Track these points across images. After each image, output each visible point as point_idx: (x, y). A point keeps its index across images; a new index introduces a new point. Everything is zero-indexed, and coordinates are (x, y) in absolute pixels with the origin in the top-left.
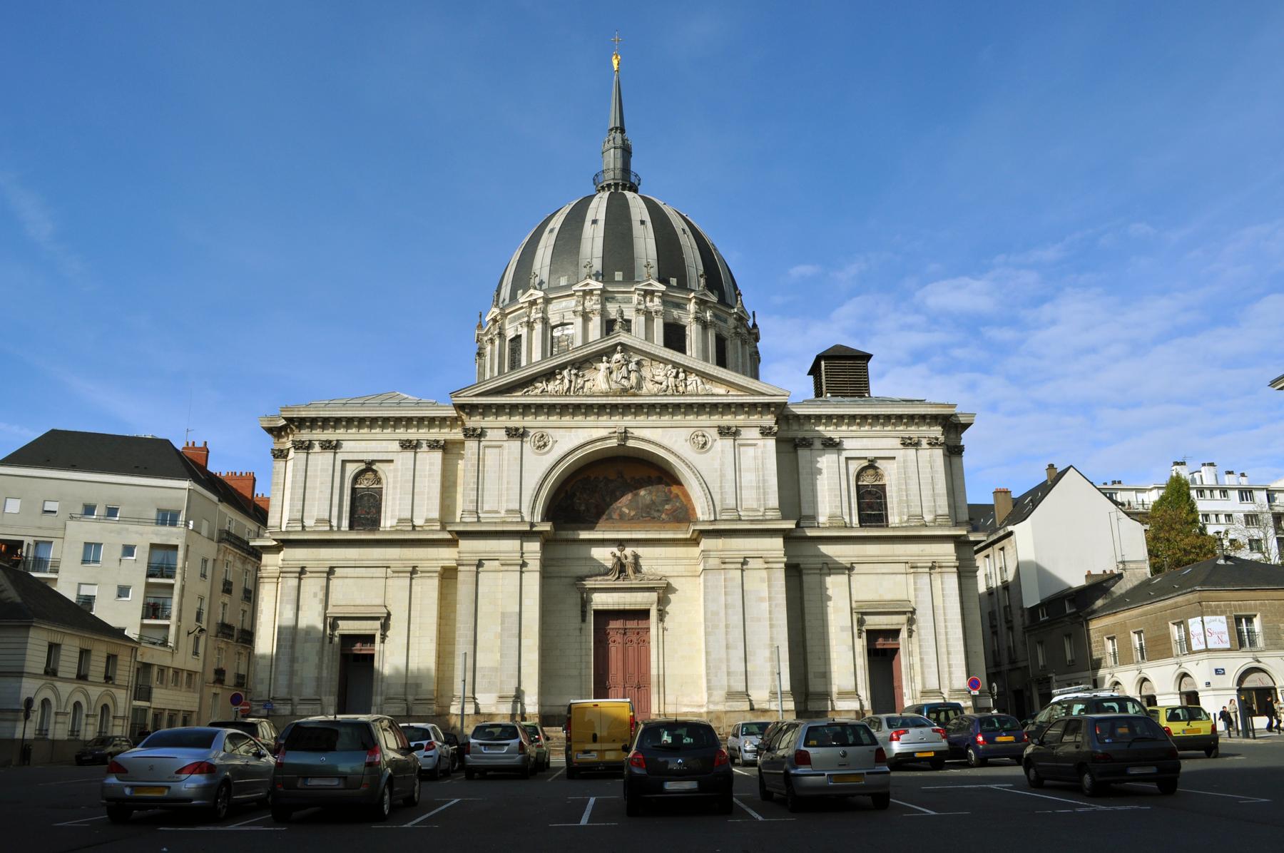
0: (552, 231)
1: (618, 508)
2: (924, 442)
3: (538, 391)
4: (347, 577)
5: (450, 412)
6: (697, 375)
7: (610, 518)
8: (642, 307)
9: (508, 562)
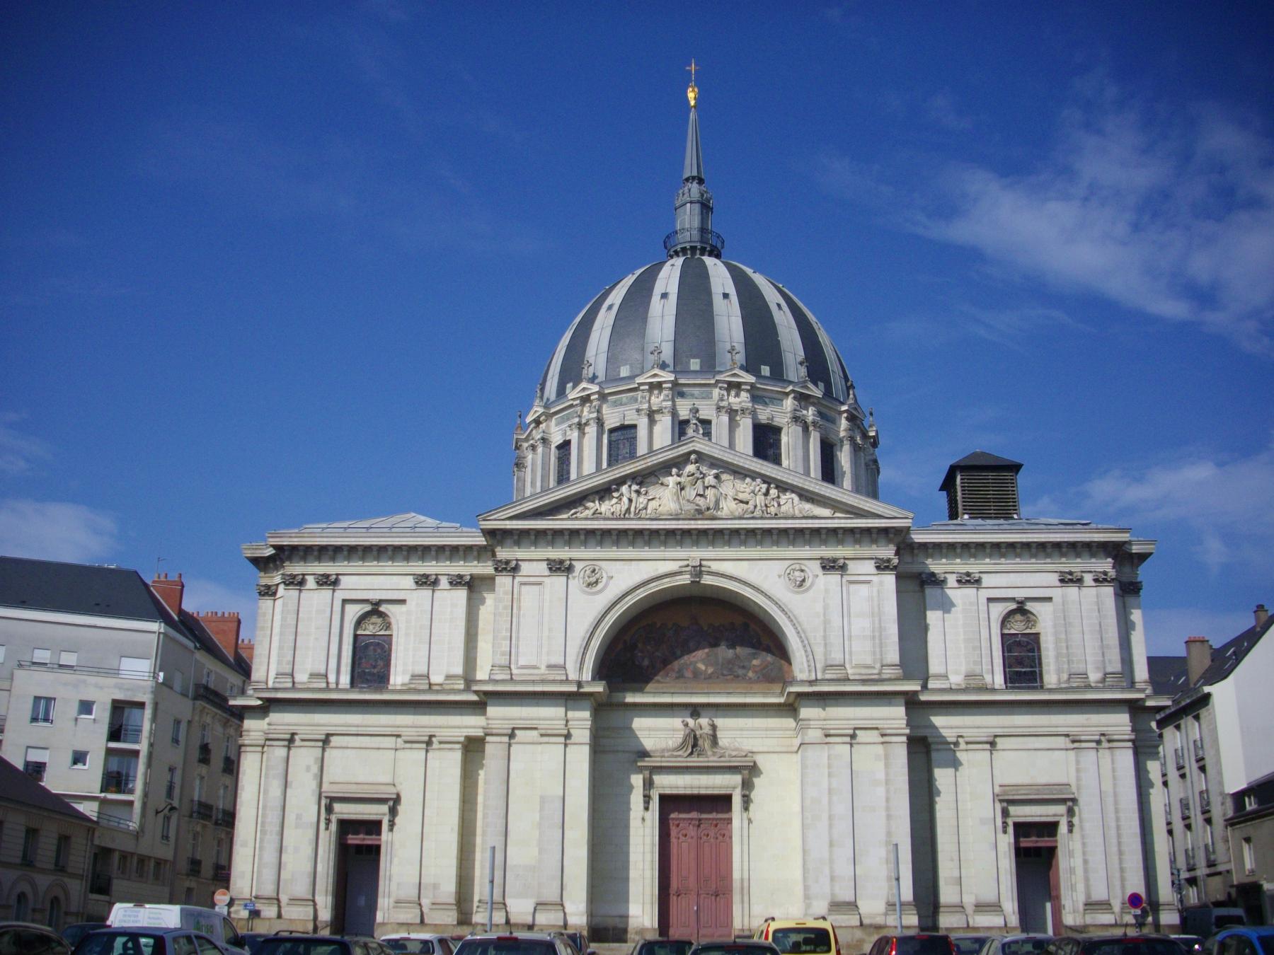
0: (610, 307)
1: (691, 663)
2: (1088, 579)
3: (588, 513)
4: (347, 748)
5: (478, 539)
6: (793, 492)
7: (680, 676)
8: (724, 404)
9: (549, 732)
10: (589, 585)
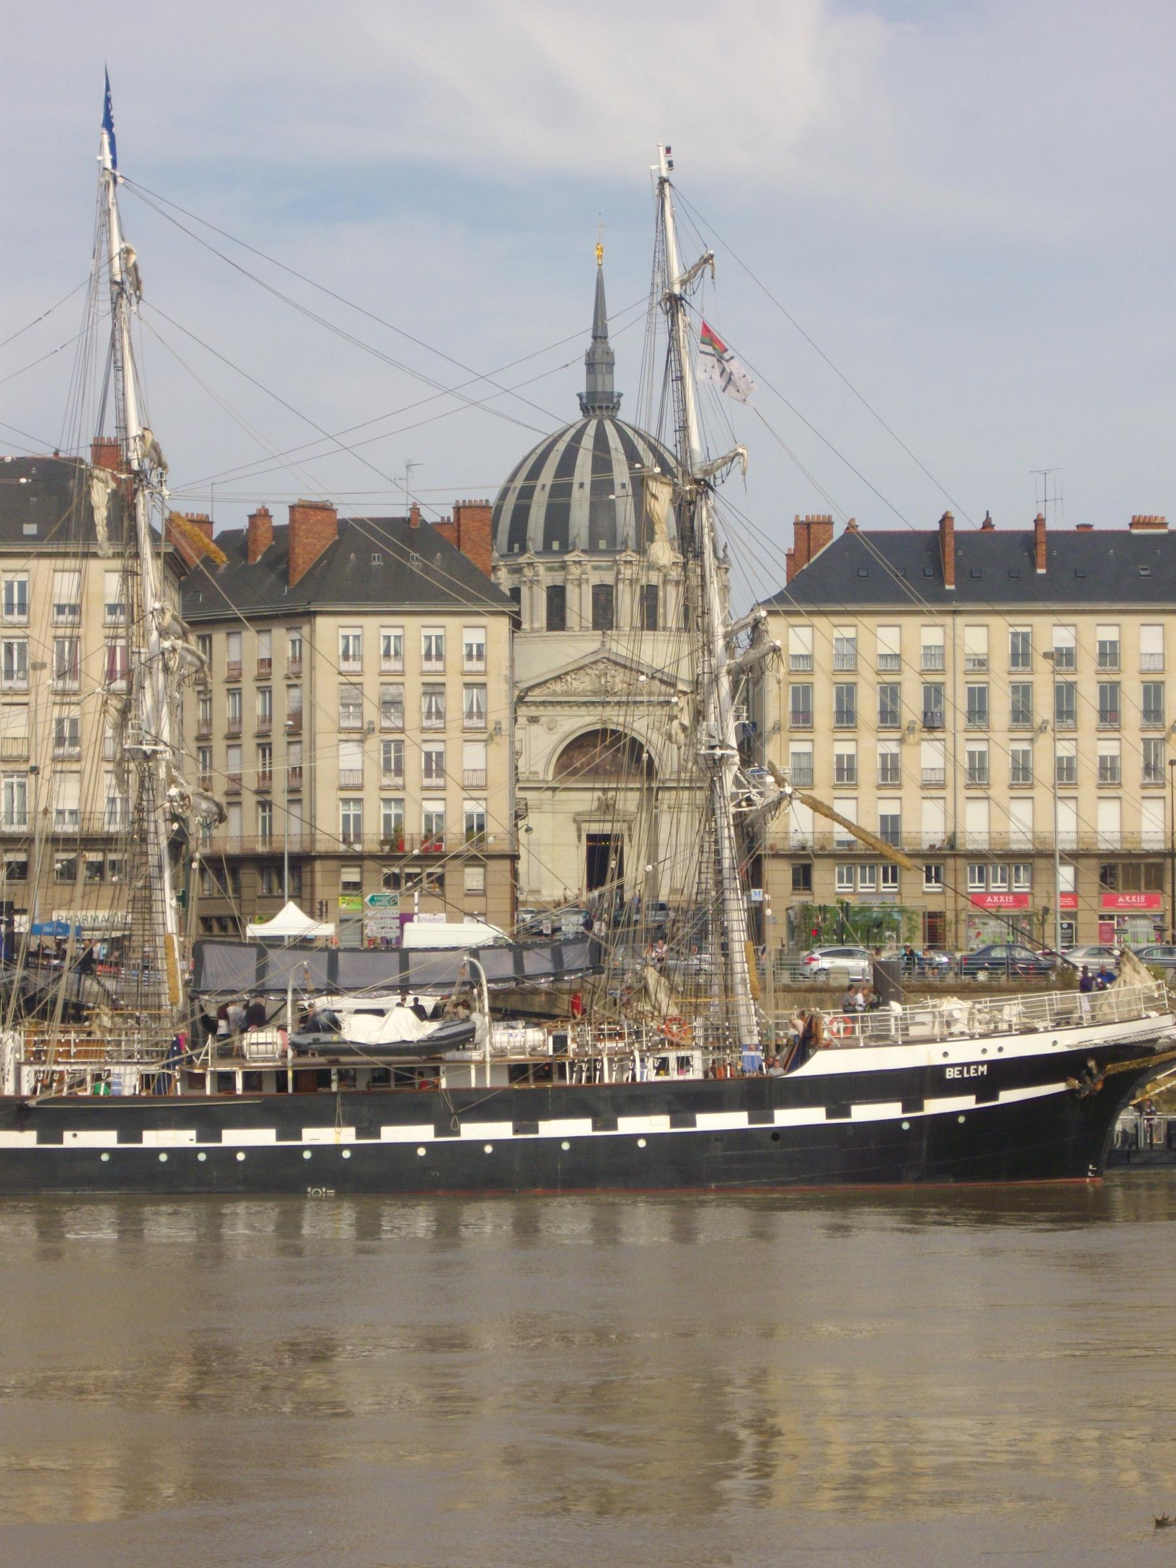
10: (550, 729)
